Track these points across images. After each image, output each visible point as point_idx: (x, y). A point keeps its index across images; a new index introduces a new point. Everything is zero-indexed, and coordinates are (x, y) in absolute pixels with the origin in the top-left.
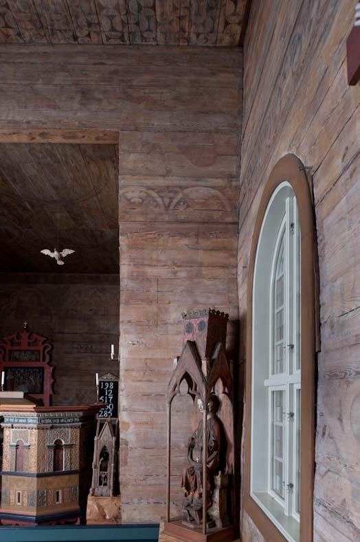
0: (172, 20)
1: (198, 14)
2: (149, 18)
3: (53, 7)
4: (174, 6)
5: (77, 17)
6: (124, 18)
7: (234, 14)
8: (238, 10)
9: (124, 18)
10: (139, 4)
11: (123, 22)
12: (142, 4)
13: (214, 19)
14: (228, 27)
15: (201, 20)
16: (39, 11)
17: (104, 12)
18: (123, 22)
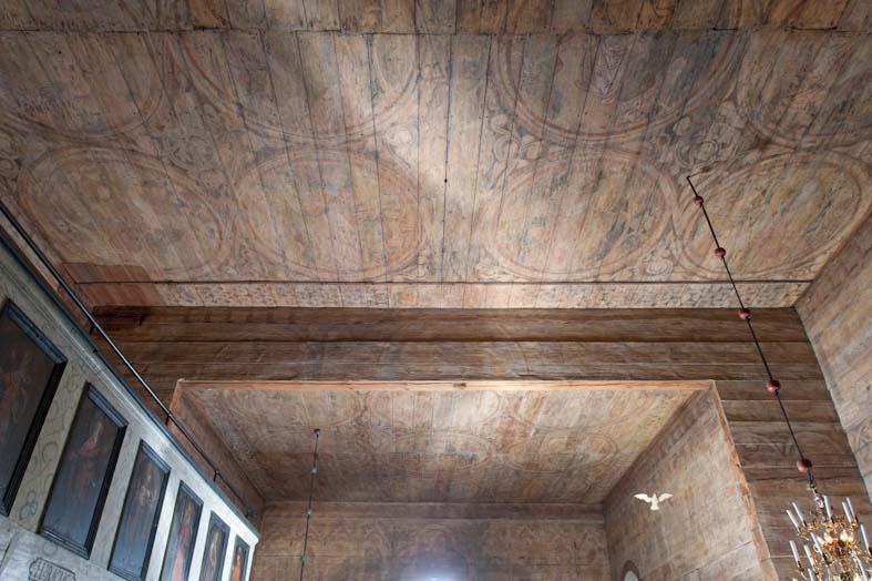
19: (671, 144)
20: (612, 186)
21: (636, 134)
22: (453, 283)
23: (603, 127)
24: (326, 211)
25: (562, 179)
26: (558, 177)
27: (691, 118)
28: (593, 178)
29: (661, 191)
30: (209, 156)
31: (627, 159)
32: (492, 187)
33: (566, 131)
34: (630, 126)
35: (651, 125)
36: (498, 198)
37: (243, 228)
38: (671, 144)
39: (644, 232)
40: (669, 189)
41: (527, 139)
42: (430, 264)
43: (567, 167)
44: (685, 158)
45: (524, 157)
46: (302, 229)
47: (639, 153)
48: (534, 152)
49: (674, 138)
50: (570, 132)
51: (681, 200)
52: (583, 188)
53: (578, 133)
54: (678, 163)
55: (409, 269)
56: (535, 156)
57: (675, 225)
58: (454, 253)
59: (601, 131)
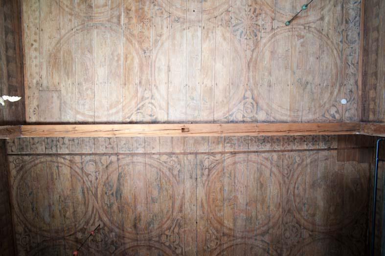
0: (38, 143)
1: (27, 146)
2: (48, 144)
3: (88, 148)
4: (37, 149)
5: (78, 143)
6: (58, 143)
7: (11, 147)
8: (10, 148)
9: (58, 143)
10: (52, 149)
11: (59, 142)
12: (50, 150)
13: (20, 144)
14: (12, 141)
15: (26, 143)
16: (94, 146)
17: (66, 146)
18: (59, 142)
19: (113, 241)
20: (129, 221)
21: (128, 246)
22: (190, 153)
23: (140, 249)
24: (247, 205)
25: (150, 225)
26: (152, 226)
27: (110, 253)
28: (138, 225)
29: (108, 218)
30: (286, 230)
31: (127, 235)
32: (178, 220)
33: (154, 247)
34: (131, 249)
35: (123, 249)
36: (174, 214)
37: (284, 190)
38: (113, 241)
39: (106, 193)
40: (105, 219)
41: (167, 244)
42: (202, 169)
43: (149, 231)
44: (105, 236)
45: (167, 236)
46: (259, 192)
47: (124, 237)
48: (163, 238)
49: (112, 243)
50: (153, 247)
51: (97, 213)
52: (140, 220)
53: (150, 246)
54: (107, 233)
55: (213, 165)
56: (163, 236)
57: (93, 197)
58: (191, 178)
59: (141, 247)
